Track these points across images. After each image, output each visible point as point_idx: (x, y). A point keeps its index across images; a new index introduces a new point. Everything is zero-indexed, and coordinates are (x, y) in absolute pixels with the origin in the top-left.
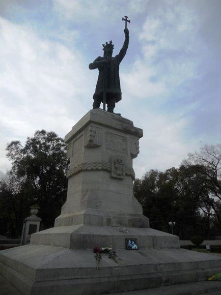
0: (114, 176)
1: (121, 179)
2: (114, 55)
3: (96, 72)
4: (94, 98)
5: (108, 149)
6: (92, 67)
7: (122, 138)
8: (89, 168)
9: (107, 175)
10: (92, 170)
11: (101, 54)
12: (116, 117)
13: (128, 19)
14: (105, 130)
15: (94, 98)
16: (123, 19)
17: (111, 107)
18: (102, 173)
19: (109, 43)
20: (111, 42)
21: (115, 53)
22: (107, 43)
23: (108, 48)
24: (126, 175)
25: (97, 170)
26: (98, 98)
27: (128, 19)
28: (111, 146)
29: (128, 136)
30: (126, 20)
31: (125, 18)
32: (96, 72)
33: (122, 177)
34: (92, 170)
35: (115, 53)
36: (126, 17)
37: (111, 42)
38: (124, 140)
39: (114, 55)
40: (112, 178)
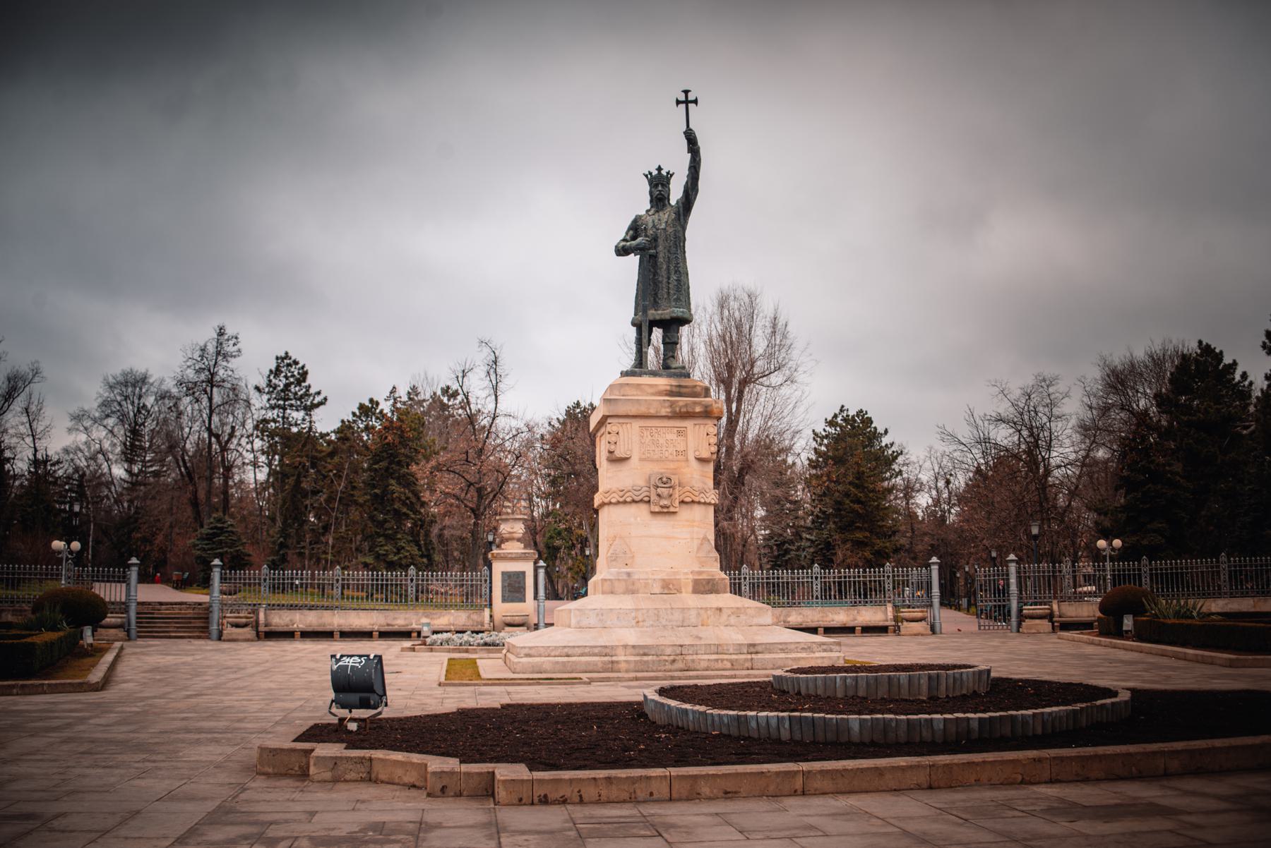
0: (657, 509)
2: (673, 202)
3: (633, 260)
4: (637, 324)
6: (622, 251)
8: (613, 501)
9: (643, 507)
10: (618, 503)
11: (641, 204)
12: (663, 388)
13: (691, 97)
14: (636, 424)
15: (633, 324)
16: (678, 102)
17: (671, 344)
18: (633, 509)
19: (655, 173)
20: (659, 169)
21: (676, 193)
23: (659, 182)
24: (682, 502)
25: (625, 502)
26: (643, 328)
27: (691, 97)
29: (689, 424)
30: (687, 101)
31: (682, 98)
32: (633, 260)
33: (672, 509)
34: (618, 503)
35: (676, 193)
36: (686, 92)
37: (659, 169)
38: (681, 433)
39: (673, 202)
40: (652, 513)
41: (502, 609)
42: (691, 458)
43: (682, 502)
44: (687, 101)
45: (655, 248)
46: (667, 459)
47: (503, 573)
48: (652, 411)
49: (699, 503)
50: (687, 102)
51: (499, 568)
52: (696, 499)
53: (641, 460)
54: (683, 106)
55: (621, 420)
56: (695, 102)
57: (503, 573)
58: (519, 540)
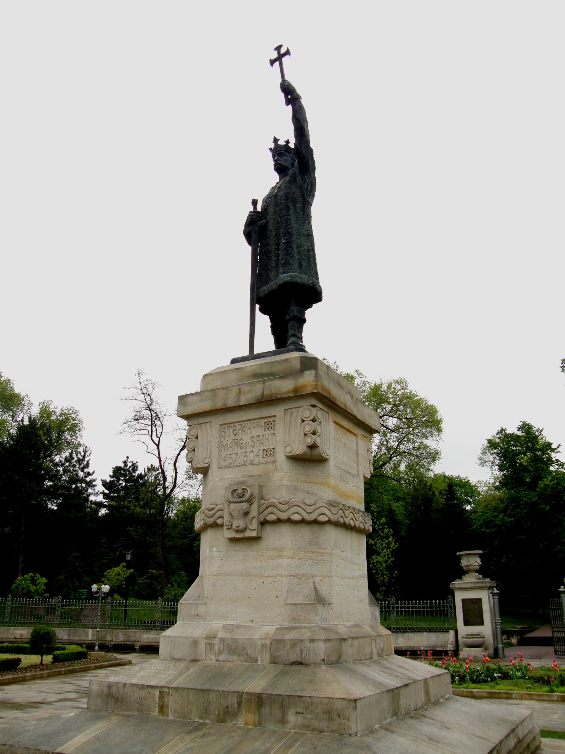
1: (257, 539)
5: (225, 467)
7: (263, 421)
13: (283, 51)
16: (272, 62)
20: (276, 140)
22: (271, 149)
27: (283, 51)
28: (234, 456)
29: (278, 411)
31: (275, 55)
33: (248, 534)
36: (278, 48)
37: (276, 140)
38: (270, 424)
41: (463, 630)
42: (280, 457)
43: (264, 523)
44: (281, 56)
45: (265, 218)
46: (252, 463)
47: (463, 600)
48: (231, 402)
49: (289, 521)
50: (280, 57)
51: (459, 597)
52: (284, 516)
53: (219, 468)
54: (277, 64)
55: (201, 420)
56: (288, 53)
57: (463, 600)
58: (477, 571)
